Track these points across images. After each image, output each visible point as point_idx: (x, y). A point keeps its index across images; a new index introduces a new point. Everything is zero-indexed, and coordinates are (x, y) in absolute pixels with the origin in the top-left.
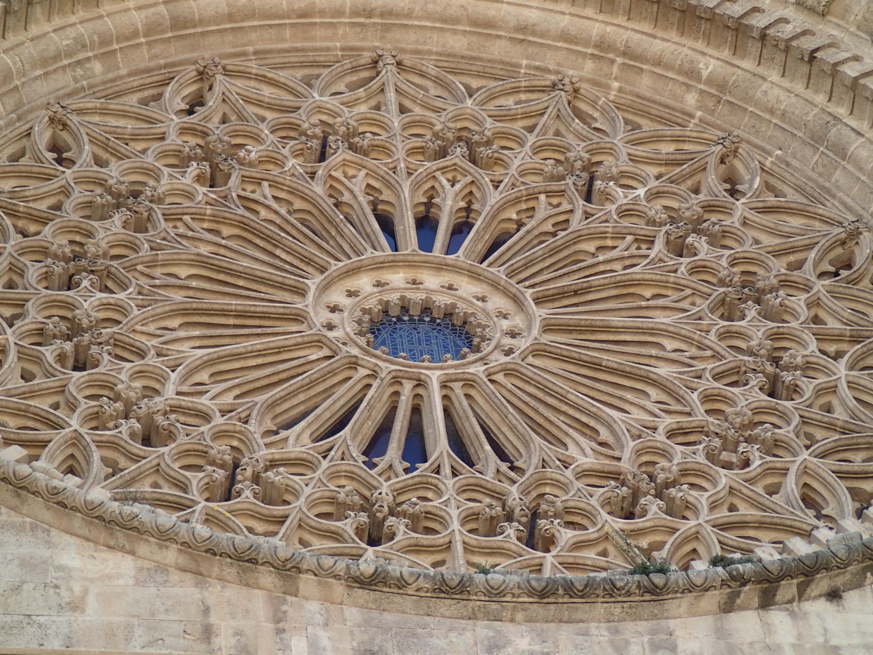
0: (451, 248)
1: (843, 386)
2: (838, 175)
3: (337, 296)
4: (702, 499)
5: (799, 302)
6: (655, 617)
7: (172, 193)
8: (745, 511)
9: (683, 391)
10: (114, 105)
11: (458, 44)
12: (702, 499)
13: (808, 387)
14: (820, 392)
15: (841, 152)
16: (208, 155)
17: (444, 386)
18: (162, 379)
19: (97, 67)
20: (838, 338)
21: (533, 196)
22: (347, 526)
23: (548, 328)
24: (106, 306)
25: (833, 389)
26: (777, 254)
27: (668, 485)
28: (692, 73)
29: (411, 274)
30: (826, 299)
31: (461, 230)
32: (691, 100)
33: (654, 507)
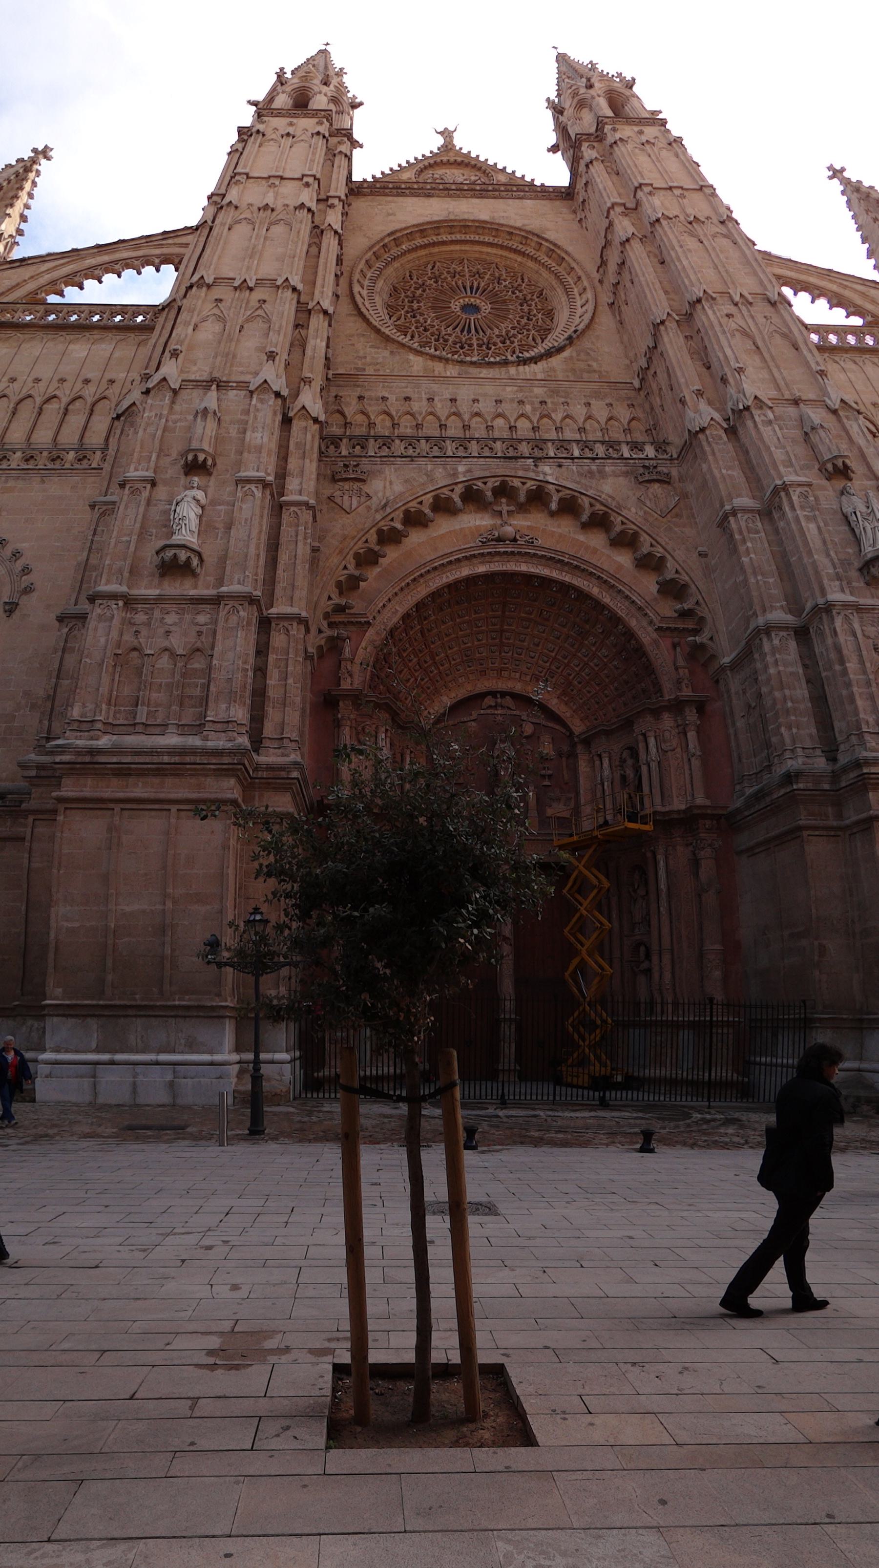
0: (476, 293)
3: (457, 303)
4: (516, 340)
8: (523, 342)
11: (477, 256)
12: (516, 340)
22: (458, 346)
31: (478, 289)
33: (508, 342)
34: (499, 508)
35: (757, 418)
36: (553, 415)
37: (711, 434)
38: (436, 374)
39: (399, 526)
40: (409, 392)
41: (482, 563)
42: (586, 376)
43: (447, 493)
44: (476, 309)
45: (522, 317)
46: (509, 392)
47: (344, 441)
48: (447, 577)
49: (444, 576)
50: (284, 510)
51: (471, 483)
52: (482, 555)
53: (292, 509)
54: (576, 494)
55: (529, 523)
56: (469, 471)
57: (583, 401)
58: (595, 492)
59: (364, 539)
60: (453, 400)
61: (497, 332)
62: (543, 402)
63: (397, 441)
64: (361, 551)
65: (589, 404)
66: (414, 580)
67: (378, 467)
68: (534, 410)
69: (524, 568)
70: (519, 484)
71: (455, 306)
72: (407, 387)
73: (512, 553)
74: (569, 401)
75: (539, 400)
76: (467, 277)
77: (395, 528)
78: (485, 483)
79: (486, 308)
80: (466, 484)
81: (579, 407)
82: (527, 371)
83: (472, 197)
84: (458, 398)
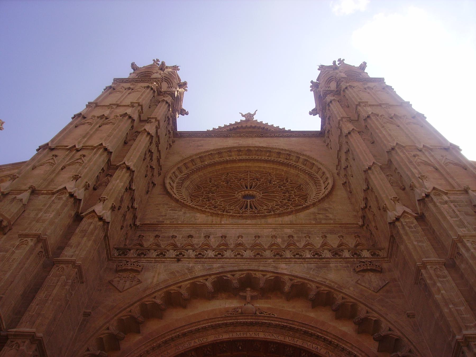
1: (297, 200)
2: (299, 179)
5: (293, 192)
6: (265, 218)
7: (222, 185)
9: (278, 201)
10: (217, 177)
11: (257, 169)
13: (292, 200)
14: (294, 201)
15: (299, 177)
16: (227, 181)
17: (250, 202)
18: (218, 202)
19: (215, 173)
20: (297, 195)
21: (263, 183)
23: (263, 196)
24: (213, 196)
25: (296, 200)
26: (291, 188)
27: (275, 210)
28: (283, 170)
29: (248, 191)
30: (296, 192)
32: (283, 173)
34: (244, 294)
35: (435, 199)
36: (298, 244)
37: (406, 222)
38: (214, 223)
39: (158, 301)
40: (192, 233)
41: (226, 332)
42: (323, 222)
43: (202, 281)
44: (253, 197)
45: (284, 199)
46: (267, 232)
47: (132, 251)
48: (195, 342)
49: (193, 341)
50: (55, 266)
51: (222, 275)
52: (226, 325)
53: (61, 265)
54: (306, 281)
55: (270, 306)
56: (222, 267)
57: (321, 235)
58: (321, 279)
59: (129, 309)
60: (224, 237)
61: (265, 208)
62: (291, 236)
63: (171, 251)
64: (124, 318)
65: (326, 237)
66: (166, 342)
67: (153, 264)
68: (284, 241)
69: (261, 335)
70: (261, 275)
71: (239, 195)
72: (191, 231)
73: (251, 324)
74: (310, 235)
75: (287, 236)
76: (249, 180)
77: (155, 303)
78: (233, 275)
79: (259, 195)
80: (219, 276)
81: (317, 239)
82: (279, 220)
83: (256, 137)
84: (227, 236)
